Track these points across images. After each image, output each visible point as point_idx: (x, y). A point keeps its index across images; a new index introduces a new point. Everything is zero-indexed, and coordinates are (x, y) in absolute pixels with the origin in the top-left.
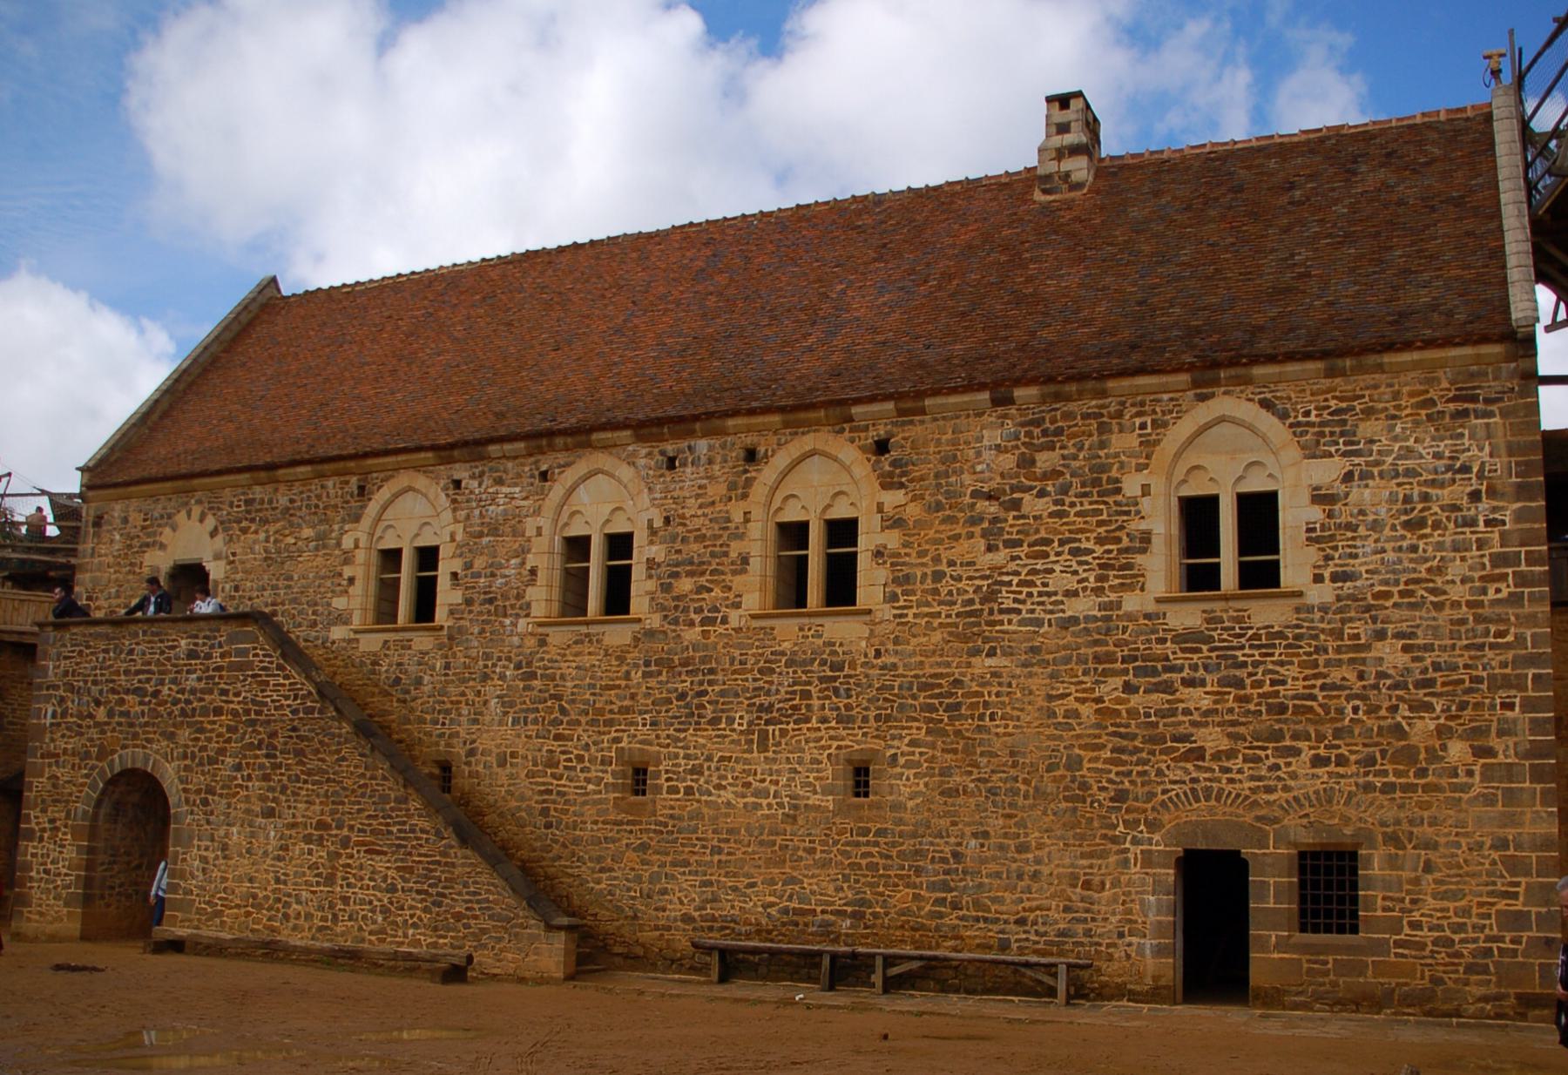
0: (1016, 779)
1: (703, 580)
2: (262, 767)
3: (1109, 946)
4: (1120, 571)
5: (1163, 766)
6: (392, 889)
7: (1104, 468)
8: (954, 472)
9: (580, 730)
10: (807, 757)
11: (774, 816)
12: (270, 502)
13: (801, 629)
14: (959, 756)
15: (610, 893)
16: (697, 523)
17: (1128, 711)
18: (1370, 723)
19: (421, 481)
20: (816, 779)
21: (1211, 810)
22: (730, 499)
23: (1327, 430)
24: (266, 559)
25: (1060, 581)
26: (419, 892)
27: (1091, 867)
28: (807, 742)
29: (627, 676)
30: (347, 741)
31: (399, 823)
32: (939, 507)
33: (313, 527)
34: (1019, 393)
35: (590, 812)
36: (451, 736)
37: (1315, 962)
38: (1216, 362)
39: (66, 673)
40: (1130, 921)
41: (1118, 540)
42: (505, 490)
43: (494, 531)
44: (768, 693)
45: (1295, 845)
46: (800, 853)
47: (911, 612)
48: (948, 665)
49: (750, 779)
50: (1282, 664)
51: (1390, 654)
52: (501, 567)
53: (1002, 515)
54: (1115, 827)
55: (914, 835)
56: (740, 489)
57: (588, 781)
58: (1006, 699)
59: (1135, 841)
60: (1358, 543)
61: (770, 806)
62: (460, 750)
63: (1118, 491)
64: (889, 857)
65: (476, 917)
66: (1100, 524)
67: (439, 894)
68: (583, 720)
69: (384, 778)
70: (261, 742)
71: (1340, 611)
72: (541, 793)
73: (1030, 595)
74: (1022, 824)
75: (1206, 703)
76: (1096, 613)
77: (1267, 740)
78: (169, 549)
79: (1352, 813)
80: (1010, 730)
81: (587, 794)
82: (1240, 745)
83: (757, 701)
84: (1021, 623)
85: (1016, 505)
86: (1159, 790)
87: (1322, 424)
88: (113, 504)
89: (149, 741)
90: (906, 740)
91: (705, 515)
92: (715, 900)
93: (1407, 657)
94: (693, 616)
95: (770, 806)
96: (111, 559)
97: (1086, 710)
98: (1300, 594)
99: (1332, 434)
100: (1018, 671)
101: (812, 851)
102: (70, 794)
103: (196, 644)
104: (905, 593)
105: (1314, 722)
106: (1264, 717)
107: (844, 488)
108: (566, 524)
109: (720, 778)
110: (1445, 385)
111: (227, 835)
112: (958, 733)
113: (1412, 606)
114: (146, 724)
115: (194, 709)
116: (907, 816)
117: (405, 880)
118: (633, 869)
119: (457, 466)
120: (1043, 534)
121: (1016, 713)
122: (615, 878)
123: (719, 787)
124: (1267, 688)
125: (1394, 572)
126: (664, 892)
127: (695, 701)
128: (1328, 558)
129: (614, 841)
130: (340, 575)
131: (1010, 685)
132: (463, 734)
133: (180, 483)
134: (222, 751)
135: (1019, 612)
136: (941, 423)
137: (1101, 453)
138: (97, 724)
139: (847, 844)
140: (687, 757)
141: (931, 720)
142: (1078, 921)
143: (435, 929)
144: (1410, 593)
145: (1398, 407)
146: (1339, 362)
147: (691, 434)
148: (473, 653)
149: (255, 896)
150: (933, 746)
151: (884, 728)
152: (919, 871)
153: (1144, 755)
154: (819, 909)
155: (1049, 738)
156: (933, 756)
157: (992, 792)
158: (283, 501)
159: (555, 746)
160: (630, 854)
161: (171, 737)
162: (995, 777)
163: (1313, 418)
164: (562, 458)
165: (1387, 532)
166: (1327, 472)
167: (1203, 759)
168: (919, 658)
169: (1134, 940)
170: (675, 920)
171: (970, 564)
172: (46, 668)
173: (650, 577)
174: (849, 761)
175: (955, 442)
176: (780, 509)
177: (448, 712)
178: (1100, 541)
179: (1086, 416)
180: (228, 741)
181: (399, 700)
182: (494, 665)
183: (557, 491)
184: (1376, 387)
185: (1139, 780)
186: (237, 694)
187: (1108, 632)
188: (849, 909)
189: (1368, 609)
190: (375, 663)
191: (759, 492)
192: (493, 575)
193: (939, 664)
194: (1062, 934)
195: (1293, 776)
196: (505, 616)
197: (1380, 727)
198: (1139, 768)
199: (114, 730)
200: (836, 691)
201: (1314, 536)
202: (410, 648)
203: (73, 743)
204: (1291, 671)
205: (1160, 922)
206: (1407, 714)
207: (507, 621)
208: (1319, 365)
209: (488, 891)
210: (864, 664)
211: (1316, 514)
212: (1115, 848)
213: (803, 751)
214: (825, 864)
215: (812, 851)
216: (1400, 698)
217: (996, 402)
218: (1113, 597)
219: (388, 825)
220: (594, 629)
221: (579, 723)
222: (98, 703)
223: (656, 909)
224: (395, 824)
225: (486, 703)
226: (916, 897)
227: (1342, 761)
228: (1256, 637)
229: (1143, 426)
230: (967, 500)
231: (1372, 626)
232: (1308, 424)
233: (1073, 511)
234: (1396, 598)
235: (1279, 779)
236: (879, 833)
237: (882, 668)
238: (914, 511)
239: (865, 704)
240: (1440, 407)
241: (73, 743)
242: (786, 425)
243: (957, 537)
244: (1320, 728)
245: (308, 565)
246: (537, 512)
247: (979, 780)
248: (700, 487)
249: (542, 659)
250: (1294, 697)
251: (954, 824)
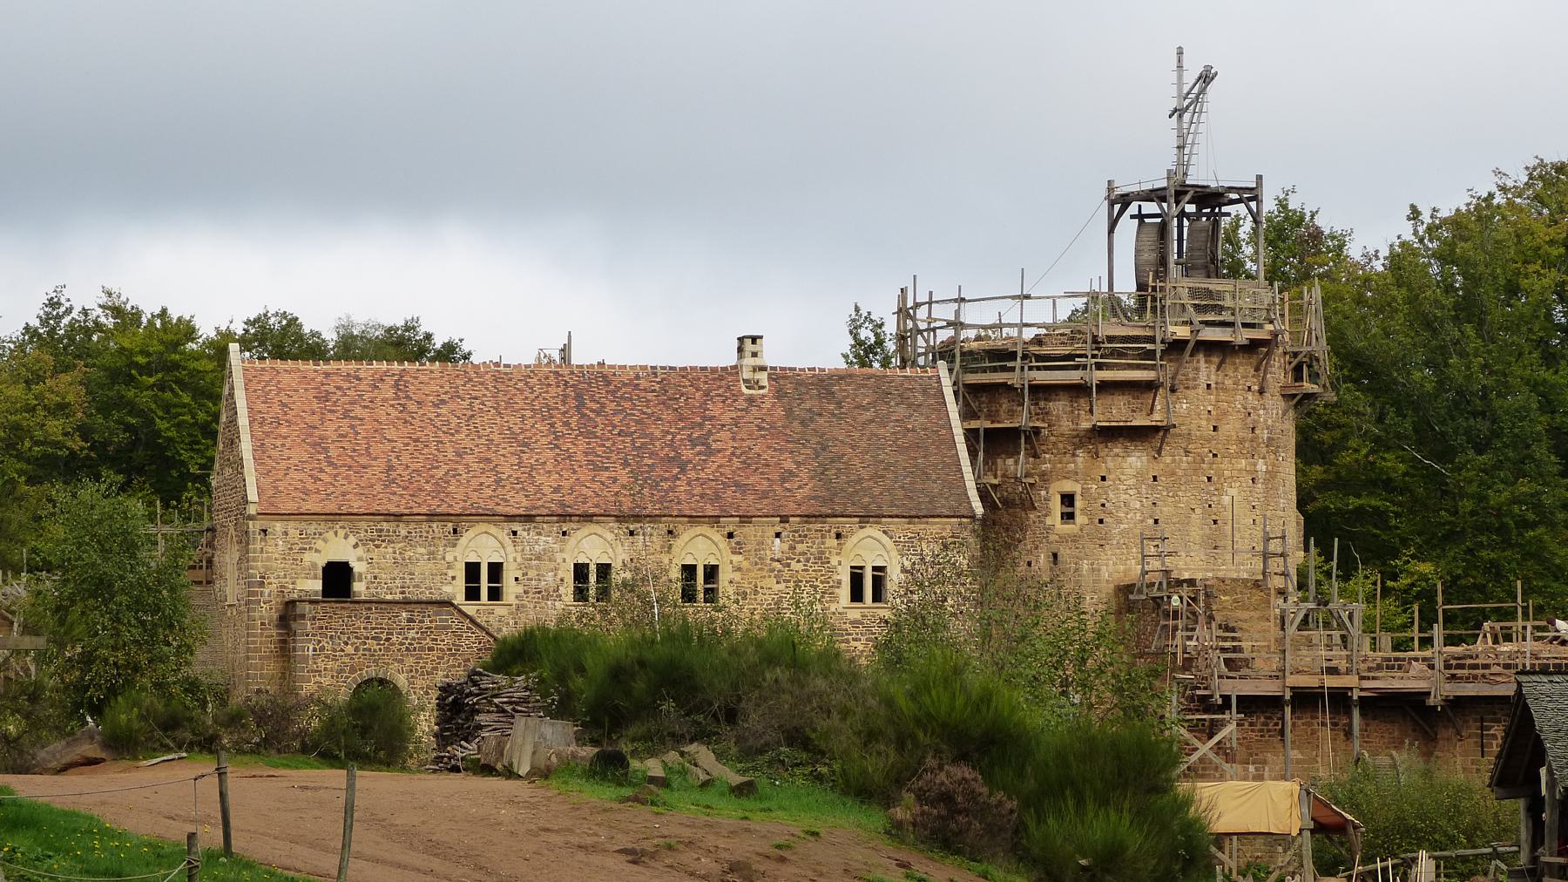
4: (830, 593)
19: (493, 529)
43: (538, 558)
85: (788, 565)
134: (436, 669)
161: (400, 661)
183: (572, 541)
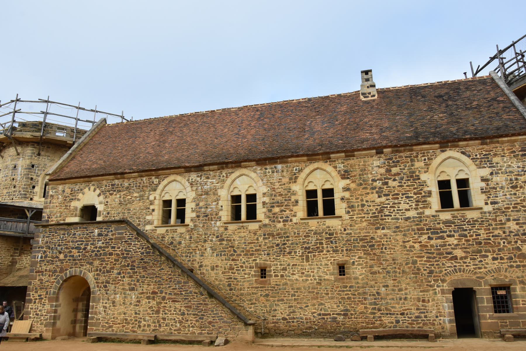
0: (395, 268)
1: (283, 208)
2: (129, 273)
3: (433, 320)
5: (444, 262)
6: (183, 314)
7: (414, 172)
8: (365, 174)
9: (241, 257)
10: (323, 263)
11: (313, 283)
12: (121, 185)
13: (318, 223)
14: (376, 261)
15: (255, 312)
16: (279, 190)
17: (431, 246)
18: (509, 246)
19: (179, 178)
20: (327, 270)
21: (461, 275)
22: (290, 183)
23: (483, 160)
24: (120, 204)
25: (403, 206)
26: (194, 315)
27: (424, 295)
28: (323, 258)
29: (257, 239)
30: (163, 263)
31: (186, 291)
32: (361, 184)
33: (138, 193)
34: (385, 150)
35: (246, 285)
36: (193, 261)
37: (503, 322)
38: (446, 142)
39: (47, 242)
40: (440, 312)
41: (421, 194)
42: (210, 180)
43: (207, 193)
44: (308, 243)
45: (490, 285)
46: (323, 295)
47: (355, 217)
48: (369, 233)
49: (304, 271)
50: (478, 229)
51: (512, 226)
52: (210, 205)
53: (382, 186)
54: (430, 282)
55: (363, 287)
56: (294, 179)
57: (245, 274)
58: (390, 243)
59: (438, 286)
60: (498, 193)
61: (311, 280)
62: (196, 265)
63: (419, 179)
64: (354, 295)
65: (217, 322)
66: (415, 189)
67: (202, 315)
68: (242, 254)
69: (179, 275)
70: (128, 265)
71: (495, 213)
72: (228, 279)
73: (394, 210)
74: (399, 282)
75: (456, 242)
76: (416, 215)
77: (477, 253)
78: (81, 201)
79: (507, 274)
80: (392, 252)
81: (245, 278)
82: (468, 255)
83: (304, 246)
84: (392, 219)
85: (386, 183)
86: (444, 269)
87: (481, 158)
88: (58, 186)
89: (82, 265)
90: (357, 257)
91: (282, 188)
92: (294, 312)
93: (518, 226)
94: (280, 219)
95: (311, 280)
96: (57, 204)
97: (417, 246)
98: (481, 208)
99: (485, 161)
100: (392, 234)
101: (327, 294)
102: (48, 286)
103: (102, 231)
104: (352, 211)
105: (492, 247)
106: (475, 246)
107: (328, 179)
108: (232, 191)
109: (293, 271)
110: (517, 147)
111: (114, 298)
112: (374, 254)
113: (517, 211)
114: (81, 259)
115: (101, 254)
116: (360, 281)
117: (188, 311)
118: (263, 303)
119: (192, 173)
120: (396, 192)
121: (393, 247)
122: (257, 306)
123: (293, 274)
124: (474, 237)
125: (510, 201)
126: (275, 310)
127: (282, 247)
128: (489, 198)
129: (256, 294)
130: (149, 208)
131: (390, 238)
132: (198, 260)
133: (86, 179)
134: (112, 268)
135: (391, 216)
136: (359, 159)
137: (412, 168)
138: (60, 260)
139: (340, 291)
140: (281, 265)
141: (365, 250)
142: (422, 313)
143: (201, 328)
144: (516, 207)
145: (504, 153)
146: (486, 141)
147: (276, 163)
148: (201, 233)
149: (126, 320)
150: (366, 258)
151: (349, 253)
152: (365, 299)
153: (437, 259)
154: (331, 313)
155: (405, 254)
156: (367, 262)
157: (388, 272)
158: (126, 184)
159: (233, 263)
160: (262, 298)
161: (91, 264)
162: (388, 268)
163: (478, 157)
164: (230, 170)
165: (506, 189)
166: (485, 172)
167: (457, 259)
168: (359, 231)
169: (442, 318)
170: (280, 320)
171: (373, 201)
172: (38, 241)
173: (264, 207)
174: (338, 264)
175: (364, 165)
176: (307, 186)
177: (191, 253)
178: (415, 194)
179: (406, 157)
180: (115, 264)
181: (172, 249)
182: (208, 237)
184: (497, 148)
185: (437, 267)
186: (119, 248)
187: (421, 221)
188: (342, 313)
189: (503, 212)
190: (163, 237)
191: (300, 180)
192: (207, 208)
193: (366, 233)
194: (417, 317)
195: (487, 264)
196: (212, 220)
197: (513, 248)
198: (436, 263)
199: (67, 262)
200: (332, 242)
201: (483, 191)
202: (176, 232)
203: (50, 267)
204: (482, 232)
205: (450, 312)
206: (521, 243)
207: (213, 222)
208: (480, 141)
209: (221, 313)
210: (340, 233)
211: (483, 184)
212: (431, 289)
213: (321, 261)
214: (332, 298)
215: (327, 294)
216: (518, 239)
217: (377, 153)
218: (421, 210)
219: (181, 291)
220: (244, 224)
221: (241, 255)
222: (60, 253)
223: (273, 316)
224: (183, 291)
225: (206, 249)
226: (366, 308)
227: (502, 258)
228: (469, 221)
229: (425, 160)
230: (370, 182)
231: (505, 217)
232: (477, 158)
233: (405, 185)
234: (512, 209)
235: (482, 265)
236: (351, 287)
237: (346, 234)
238: (353, 186)
239: (342, 246)
240: (517, 153)
241: (50, 267)
242: (308, 160)
243: (368, 193)
244: (494, 249)
245: (136, 206)
246: (222, 187)
247: (383, 269)
248: (280, 179)
249: (226, 234)
250: (484, 239)
251: (376, 283)
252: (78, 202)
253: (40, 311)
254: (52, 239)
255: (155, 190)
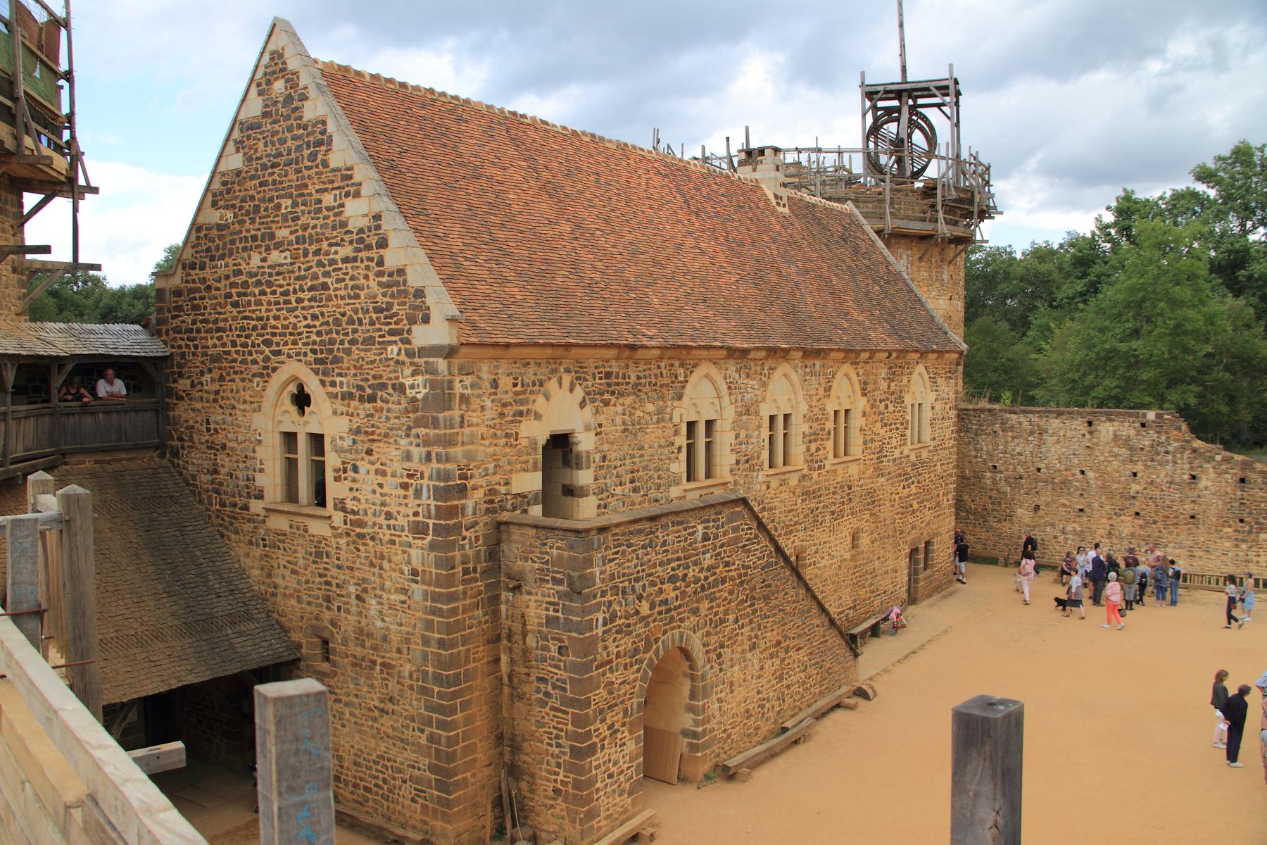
24: (624, 431)
39: (612, 577)
78: (545, 418)
89: (682, 620)
96: (483, 430)
102: (625, 694)
130: (673, 444)
134: (726, 612)
161: (695, 612)
199: (655, 621)
203: (626, 643)
222: (640, 598)
241: (626, 643)
246: (764, 400)
252: (535, 423)
253: (615, 764)
254: (620, 565)
255: (680, 398)
